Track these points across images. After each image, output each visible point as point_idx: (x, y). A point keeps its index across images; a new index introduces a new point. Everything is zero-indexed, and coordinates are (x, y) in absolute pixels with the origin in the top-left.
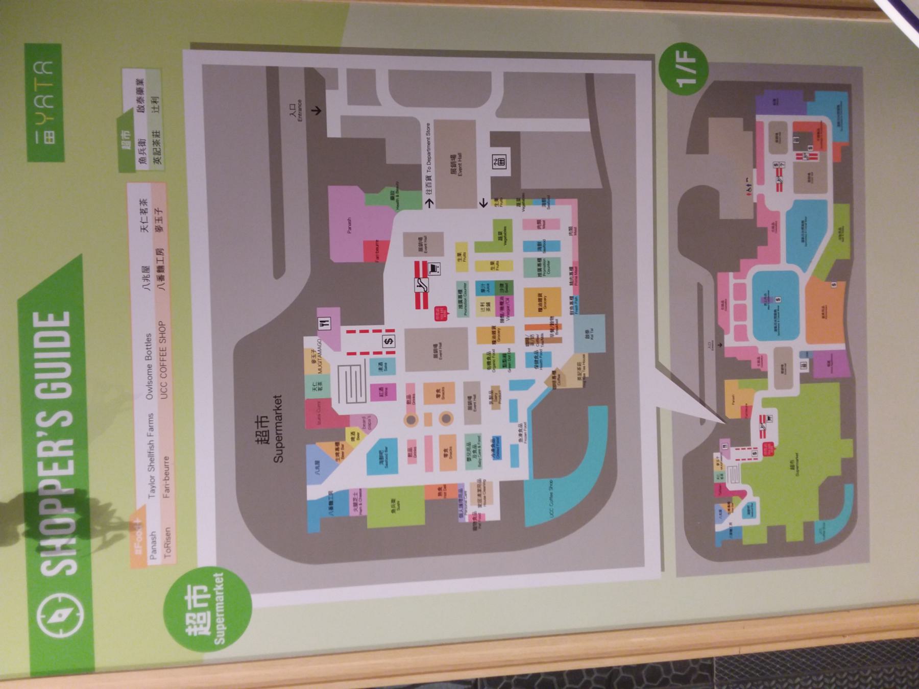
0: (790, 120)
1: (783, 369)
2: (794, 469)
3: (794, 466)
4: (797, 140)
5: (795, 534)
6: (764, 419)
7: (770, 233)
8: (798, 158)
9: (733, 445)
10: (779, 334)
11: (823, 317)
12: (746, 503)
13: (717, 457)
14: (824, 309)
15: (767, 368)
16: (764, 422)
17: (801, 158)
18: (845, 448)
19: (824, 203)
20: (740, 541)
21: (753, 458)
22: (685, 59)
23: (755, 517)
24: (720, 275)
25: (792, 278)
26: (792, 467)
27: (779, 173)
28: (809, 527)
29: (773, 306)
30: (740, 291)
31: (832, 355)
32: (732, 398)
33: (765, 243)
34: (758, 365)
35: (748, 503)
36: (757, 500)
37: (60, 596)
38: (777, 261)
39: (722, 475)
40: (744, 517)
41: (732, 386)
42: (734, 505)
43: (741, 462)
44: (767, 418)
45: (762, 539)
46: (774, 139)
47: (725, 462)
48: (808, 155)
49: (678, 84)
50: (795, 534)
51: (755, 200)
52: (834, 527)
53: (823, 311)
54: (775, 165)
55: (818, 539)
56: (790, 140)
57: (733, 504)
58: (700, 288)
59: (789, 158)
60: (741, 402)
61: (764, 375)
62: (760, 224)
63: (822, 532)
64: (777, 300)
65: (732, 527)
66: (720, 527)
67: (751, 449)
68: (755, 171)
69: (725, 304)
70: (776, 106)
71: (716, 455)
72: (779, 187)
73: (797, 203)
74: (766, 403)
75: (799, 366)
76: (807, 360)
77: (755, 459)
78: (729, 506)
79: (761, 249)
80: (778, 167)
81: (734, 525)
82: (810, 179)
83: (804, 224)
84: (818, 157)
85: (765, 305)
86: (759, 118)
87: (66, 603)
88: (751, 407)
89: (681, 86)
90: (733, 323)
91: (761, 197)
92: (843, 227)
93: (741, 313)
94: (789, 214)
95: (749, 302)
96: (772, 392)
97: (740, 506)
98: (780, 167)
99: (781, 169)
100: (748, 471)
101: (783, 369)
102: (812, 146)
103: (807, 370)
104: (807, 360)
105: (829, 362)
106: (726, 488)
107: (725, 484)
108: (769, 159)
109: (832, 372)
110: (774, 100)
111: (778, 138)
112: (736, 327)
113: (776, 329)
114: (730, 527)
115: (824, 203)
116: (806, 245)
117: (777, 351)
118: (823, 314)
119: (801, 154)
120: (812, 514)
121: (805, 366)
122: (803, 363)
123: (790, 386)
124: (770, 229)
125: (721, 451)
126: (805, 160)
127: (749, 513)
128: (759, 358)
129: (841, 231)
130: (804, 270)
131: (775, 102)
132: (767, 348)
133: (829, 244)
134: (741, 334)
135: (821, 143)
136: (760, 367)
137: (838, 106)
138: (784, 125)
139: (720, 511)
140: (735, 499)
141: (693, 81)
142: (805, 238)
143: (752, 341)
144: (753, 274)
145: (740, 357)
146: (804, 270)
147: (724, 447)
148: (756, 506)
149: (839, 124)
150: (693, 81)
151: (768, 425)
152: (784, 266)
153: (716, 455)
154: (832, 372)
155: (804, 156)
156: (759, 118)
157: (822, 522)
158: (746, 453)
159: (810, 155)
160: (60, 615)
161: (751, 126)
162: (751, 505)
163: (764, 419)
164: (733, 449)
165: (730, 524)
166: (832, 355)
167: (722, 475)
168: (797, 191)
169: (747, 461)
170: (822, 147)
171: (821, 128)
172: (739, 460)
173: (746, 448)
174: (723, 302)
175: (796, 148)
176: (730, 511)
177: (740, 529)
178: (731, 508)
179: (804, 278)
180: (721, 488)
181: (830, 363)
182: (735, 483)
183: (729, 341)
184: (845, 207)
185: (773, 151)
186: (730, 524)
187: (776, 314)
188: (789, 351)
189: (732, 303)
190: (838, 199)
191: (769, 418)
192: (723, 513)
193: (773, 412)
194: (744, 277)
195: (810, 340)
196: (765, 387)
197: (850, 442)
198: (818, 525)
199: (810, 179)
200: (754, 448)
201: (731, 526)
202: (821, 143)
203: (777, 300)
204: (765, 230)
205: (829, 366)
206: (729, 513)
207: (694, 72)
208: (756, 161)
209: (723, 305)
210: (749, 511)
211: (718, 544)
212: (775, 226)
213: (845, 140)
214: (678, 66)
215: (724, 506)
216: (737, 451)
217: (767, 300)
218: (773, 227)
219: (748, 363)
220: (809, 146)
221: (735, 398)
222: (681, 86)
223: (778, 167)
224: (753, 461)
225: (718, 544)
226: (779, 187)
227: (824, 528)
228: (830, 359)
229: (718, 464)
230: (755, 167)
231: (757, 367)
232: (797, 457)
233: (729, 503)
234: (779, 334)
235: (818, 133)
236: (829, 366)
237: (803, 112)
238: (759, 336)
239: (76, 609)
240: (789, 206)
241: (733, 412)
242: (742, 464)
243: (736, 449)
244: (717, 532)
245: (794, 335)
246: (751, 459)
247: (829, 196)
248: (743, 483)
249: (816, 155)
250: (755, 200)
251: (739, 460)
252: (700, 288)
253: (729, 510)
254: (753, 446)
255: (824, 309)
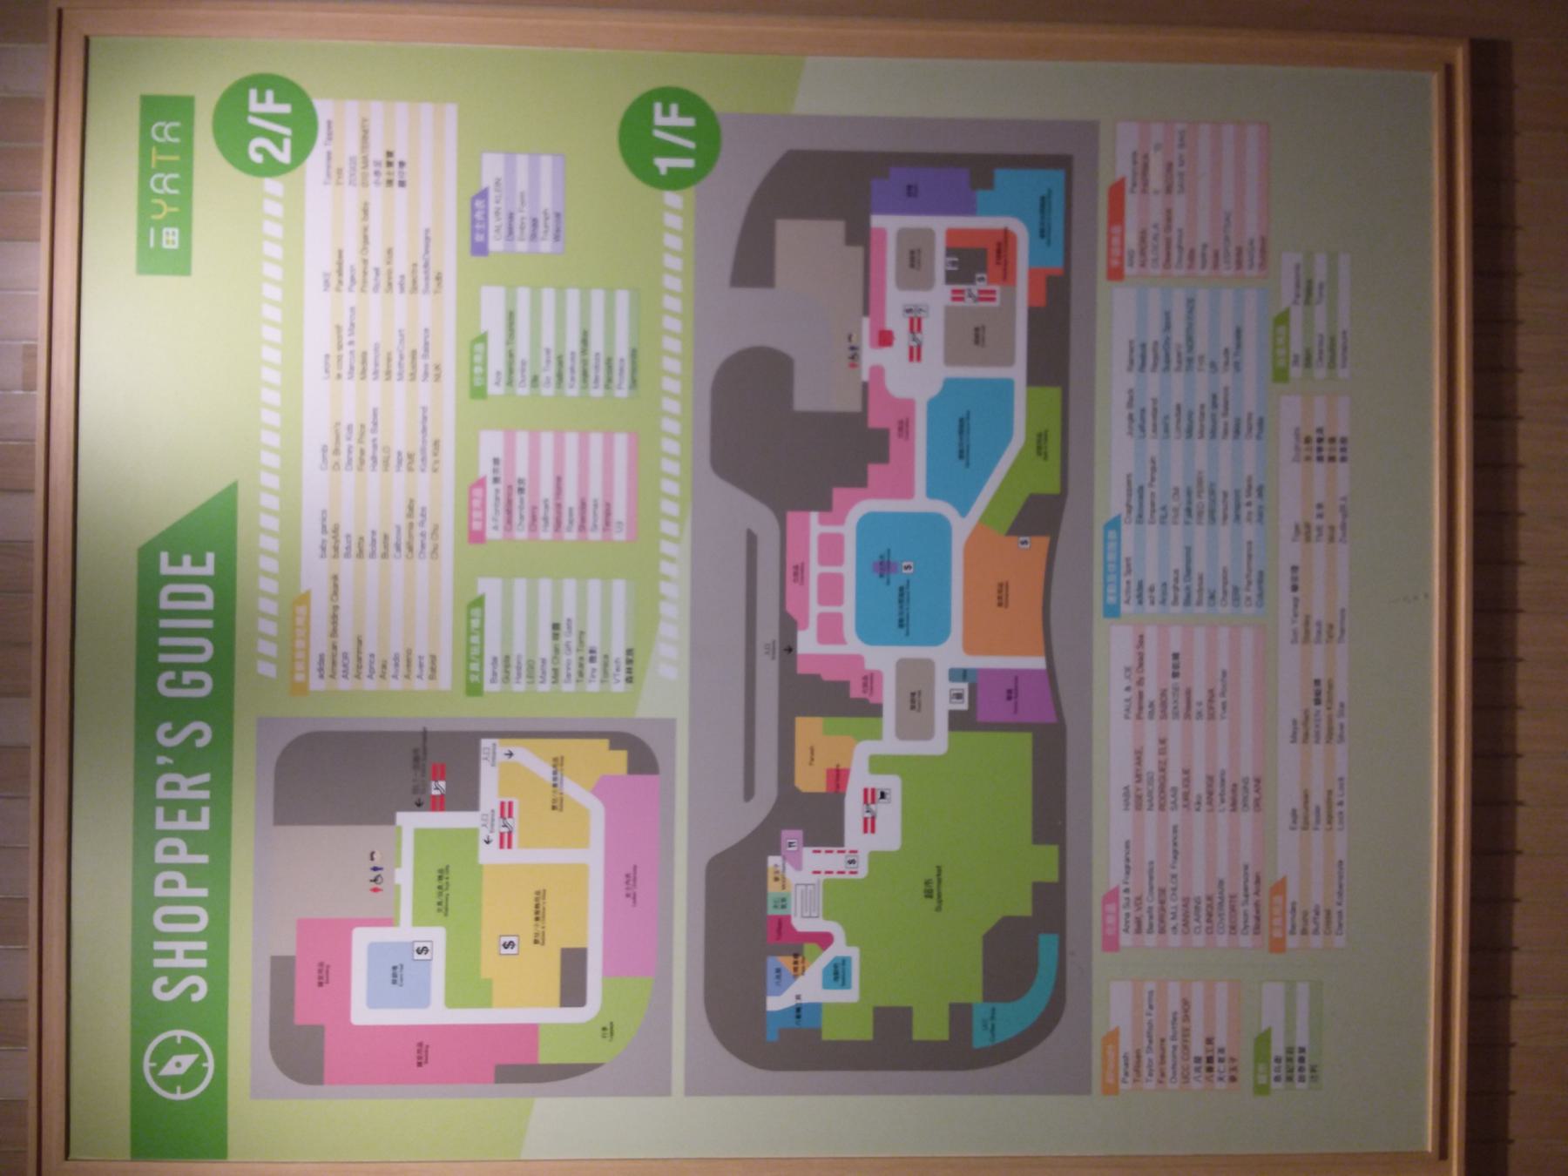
0: (940, 225)
1: (915, 701)
2: (931, 897)
3: (932, 891)
4: (954, 263)
5: (930, 1026)
6: (872, 796)
7: (895, 442)
8: (954, 299)
9: (807, 843)
10: (907, 634)
11: (1000, 605)
12: (831, 959)
13: (776, 866)
14: (1003, 588)
15: (880, 694)
16: (873, 802)
17: (961, 299)
18: (1043, 863)
19: (1008, 384)
20: (817, 1032)
21: (847, 870)
22: (675, 120)
23: (849, 987)
24: (792, 516)
25: (940, 527)
26: (929, 894)
27: (915, 326)
28: (960, 1015)
29: (897, 580)
30: (832, 550)
31: (1016, 679)
32: (809, 752)
33: (883, 458)
34: (865, 692)
35: (836, 958)
36: (854, 953)
37: (179, 1034)
38: (908, 493)
39: (784, 900)
40: (826, 986)
41: (808, 729)
42: (806, 961)
43: (823, 877)
44: (878, 795)
45: (863, 1031)
46: (907, 261)
47: (791, 875)
48: (975, 293)
49: (656, 169)
50: (930, 1026)
51: (865, 376)
52: (1015, 1017)
53: (1000, 591)
54: (909, 311)
55: (981, 1040)
56: (940, 263)
57: (804, 959)
58: (752, 539)
59: (937, 298)
60: (825, 762)
61: (876, 711)
62: (874, 422)
63: (989, 1026)
64: (906, 568)
65: (801, 1004)
66: (775, 1003)
67: (843, 852)
68: (866, 322)
69: (800, 572)
70: (911, 199)
71: (773, 861)
72: (915, 354)
73: (949, 384)
74: (879, 764)
75: (947, 698)
76: (963, 687)
77: (852, 873)
78: (796, 963)
79: (874, 470)
80: (912, 315)
81: (805, 1000)
82: (978, 337)
83: (963, 426)
84: (998, 296)
85: (881, 576)
86: (877, 221)
87: (189, 1047)
88: (847, 772)
89: (663, 172)
90: (815, 609)
91: (878, 372)
92: (1046, 432)
93: (831, 589)
94: (933, 405)
95: (848, 570)
96: (889, 743)
97: (819, 963)
98: (919, 315)
99: (919, 320)
100: (836, 895)
101: (915, 701)
102: (985, 276)
103: (963, 706)
104: (963, 687)
105: (1009, 691)
106: (792, 929)
107: (788, 918)
108: (896, 301)
109: (1016, 711)
110: (909, 187)
111: (914, 259)
112: (821, 617)
113: (901, 624)
114: (797, 1004)
115: (1008, 384)
116: (968, 464)
117: (903, 666)
118: (999, 598)
119: (961, 291)
120: (971, 992)
121: (959, 696)
122: (955, 692)
123: (927, 733)
124: (894, 432)
125: (783, 853)
126: (968, 302)
127: (836, 979)
128: (865, 678)
129: (1039, 443)
130: (963, 511)
131: (911, 191)
132: (883, 659)
133: (1014, 467)
134: (830, 630)
135: (1005, 270)
136: (867, 696)
137: (1043, 199)
138: (929, 234)
139: (778, 971)
140: (809, 948)
141: (688, 163)
142: (965, 448)
143: (853, 644)
144: (865, 512)
145: (827, 676)
146: (963, 511)
147: (790, 846)
148: (850, 965)
149: (1044, 233)
150: (688, 163)
151: (881, 808)
152: (920, 503)
153: (773, 861)
154: (1016, 711)
155: (966, 294)
156: (877, 221)
157: (989, 1005)
158: (831, 860)
159: (981, 292)
160: (178, 1065)
161: (859, 235)
162: (840, 961)
163: (872, 796)
164: (807, 852)
165: (798, 997)
166: (1016, 679)
167: (784, 900)
168: (951, 358)
169: (835, 876)
170: (1007, 276)
171: (1004, 243)
172: (818, 872)
173: (835, 849)
174: (796, 567)
175: (950, 278)
176: (797, 972)
177: (817, 1008)
178: (800, 966)
179: (962, 528)
180: (782, 925)
181: (1010, 695)
182: (810, 917)
183: (807, 643)
184: (1054, 393)
185: (903, 284)
186: (798, 997)
187: (902, 592)
188: (927, 666)
189: (815, 570)
190: (1036, 377)
191: (883, 795)
192: (784, 977)
193: (891, 782)
194: (840, 521)
195: (970, 648)
196: (878, 736)
197: (1052, 851)
198: (981, 1011)
199: (978, 337)
200: (852, 852)
201: (799, 1001)
202: (1005, 270)
203: (906, 568)
204: (883, 435)
205: (1009, 698)
206: (796, 977)
207: (691, 145)
208: (870, 302)
209: (795, 574)
210: (836, 973)
211: (772, 1036)
212: (905, 427)
213: (1055, 262)
214: (658, 134)
215: (786, 962)
216: (829, 854)
217: (884, 567)
218: (900, 429)
219: (845, 686)
220: (978, 276)
221: (815, 753)
222: (663, 172)
223: (912, 315)
224: (847, 876)
225: (772, 1036)
226: (915, 354)
227: (993, 1018)
228: (1013, 686)
229: (776, 879)
230: (866, 312)
231: (862, 696)
232: (939, 875)
233: (796, 955)
234: (907, 634)
235: (999, 252)
236: (1009, 698)
237: (969, 209)
238: (868, 634)
239: (203, 1058)
240: (935, 389)
241: (810, 780)
242: (826, 881)
243: (815, 852)
244: (773, 1013)
245: (938, 635)
246: (842, 873)
247: (1017, 372)
248: (827, 917)
249: (993, 292)
250: (865, 376)
251: (818, 872)
252: (752, 539)
253: (795, 969)
254: (849, 845)
255: (1003, 588)
